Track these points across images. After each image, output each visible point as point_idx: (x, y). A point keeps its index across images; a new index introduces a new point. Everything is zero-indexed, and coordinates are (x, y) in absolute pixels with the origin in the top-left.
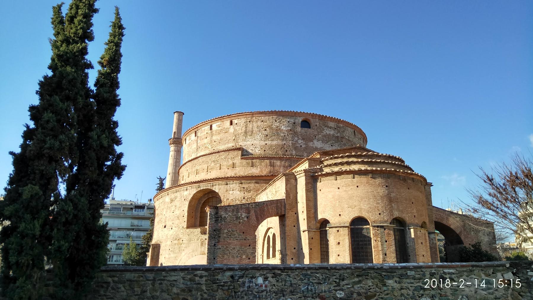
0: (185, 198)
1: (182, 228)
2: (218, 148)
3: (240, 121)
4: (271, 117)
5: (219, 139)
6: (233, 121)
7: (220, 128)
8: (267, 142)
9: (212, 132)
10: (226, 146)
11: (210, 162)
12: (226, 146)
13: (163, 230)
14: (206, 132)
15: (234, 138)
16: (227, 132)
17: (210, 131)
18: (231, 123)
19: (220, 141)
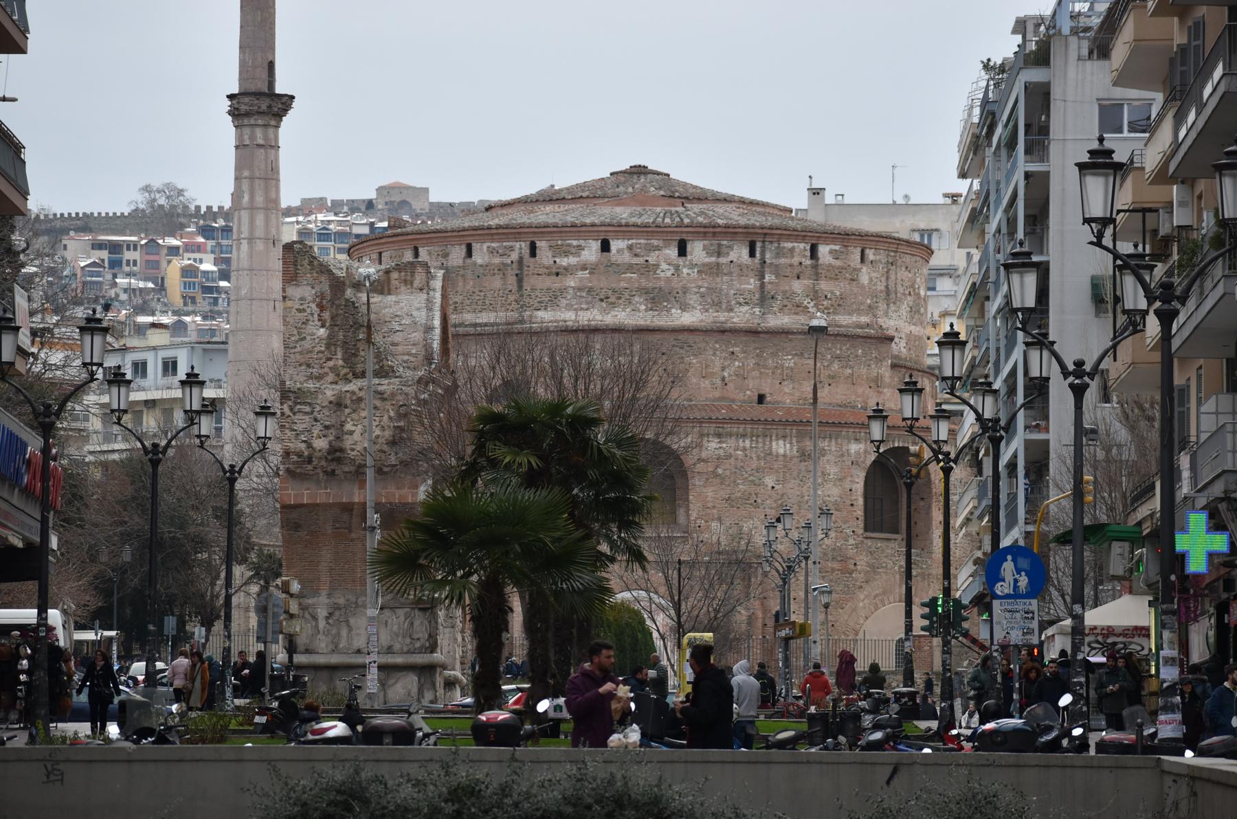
0: (853, 458)
2: (837, 318)
3: (878, 257)
4: (914, 258)
5: (838, 293)
6: (867, 251)
7: (838, 263)
8: (913, 328)
9: (815, 267)
10: (854, 318)
11: (829, 356)
12: (854, 318)
14: (796, 260)
15: (869, 301)
16: (853, 280)
17: (809, 262)
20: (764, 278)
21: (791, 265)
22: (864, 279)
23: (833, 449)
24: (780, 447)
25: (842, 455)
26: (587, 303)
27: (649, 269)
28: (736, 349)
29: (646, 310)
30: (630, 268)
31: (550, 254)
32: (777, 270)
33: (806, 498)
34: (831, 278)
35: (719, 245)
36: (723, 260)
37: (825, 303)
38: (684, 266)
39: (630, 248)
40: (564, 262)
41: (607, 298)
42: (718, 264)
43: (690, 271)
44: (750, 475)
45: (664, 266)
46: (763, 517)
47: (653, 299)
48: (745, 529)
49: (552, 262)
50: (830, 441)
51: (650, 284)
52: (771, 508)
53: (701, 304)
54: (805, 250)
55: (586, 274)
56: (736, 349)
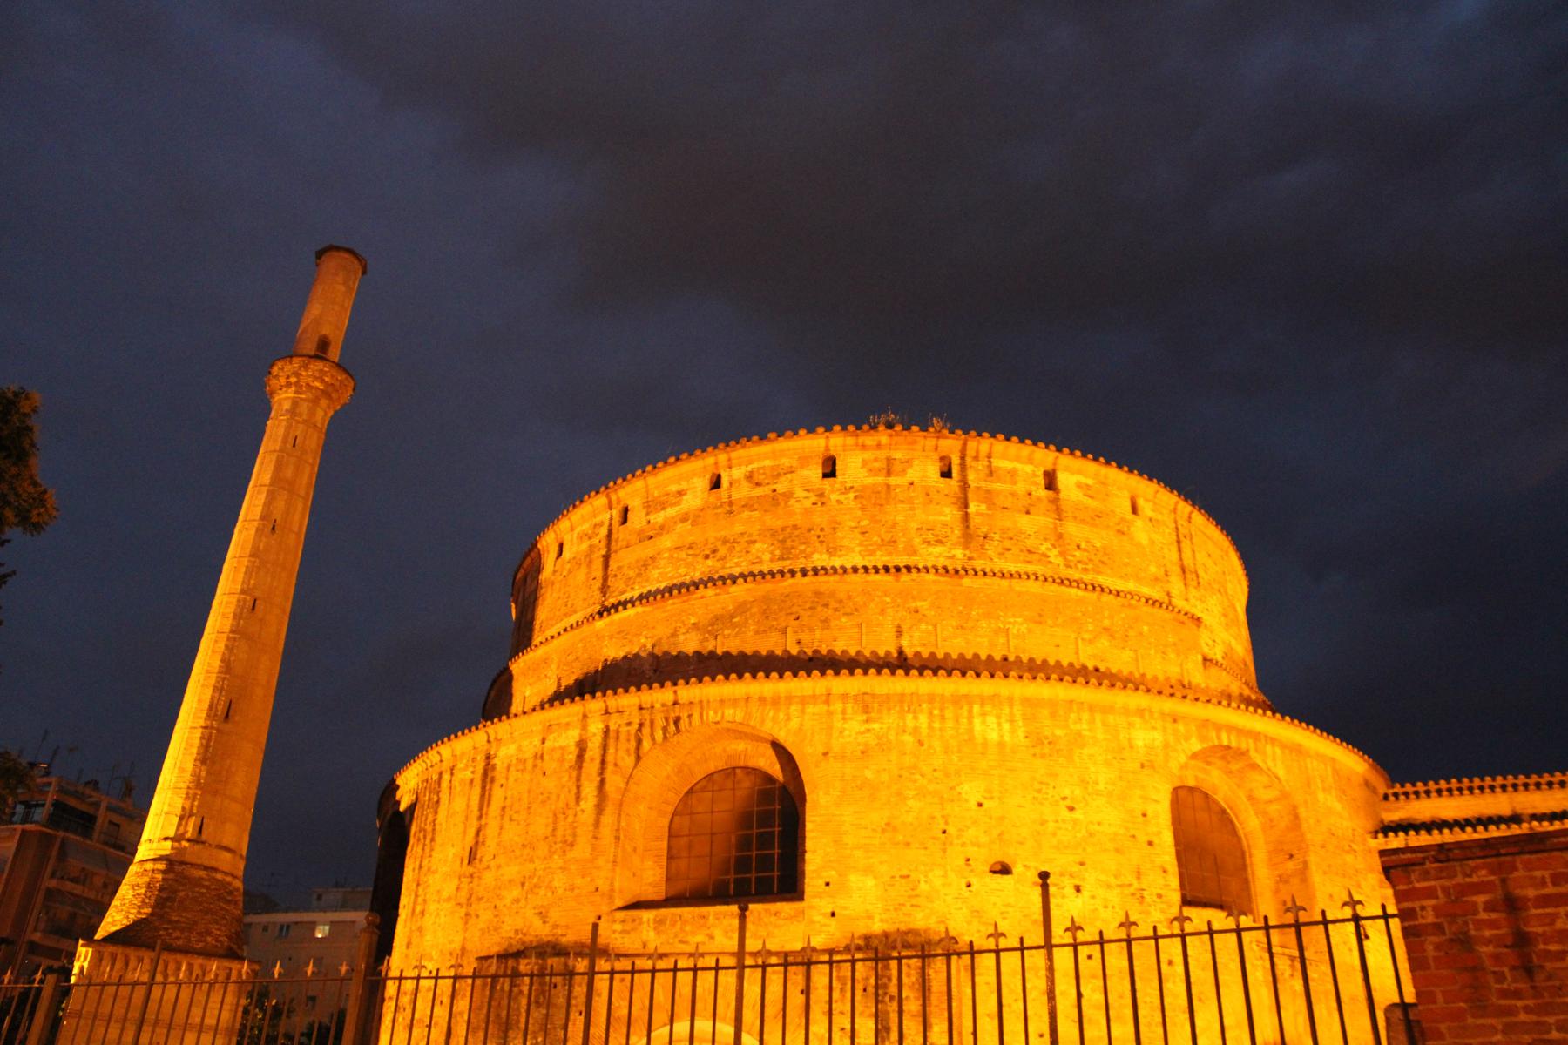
1: (1155, 898)
9: (1055, 502)
13: (974, 881)
14: (1021, 488)
16: (1123, 533)
18: (1135, 510)
19: (1104, 559)
20: (966, 506)
21: (1013, 494)
22: (1140, 530)
23: (1100, 736)
24: (990, 728)
25: (1122, 749)
26: (688, 565)
27: (777, 500)
28: (919, 604)
29: (772, 560)
30: (748, 505)
31: (644, 512)
32: (988, 497)
33: (1051, 826)
34: (1083, 521)
35: (889, 460)
36: (893, 480)
37: (1078, 554)
38: (832, 491)
39: (749, 477)
40: (659, 518)
41: (714, 551)
42: (888, 486)
43: (842, 498)
44: (930, 781)
45: (800, 493)
46: (962, 862)
47: (783, 542)
48: (923, 886)
49: (644, 523)
50: (1092, 721)
51: (779, 523)
52: (978, 845)
53: (861, 544)
54: (1034, 475)
55: (687, 525)
56: (919, 604)
